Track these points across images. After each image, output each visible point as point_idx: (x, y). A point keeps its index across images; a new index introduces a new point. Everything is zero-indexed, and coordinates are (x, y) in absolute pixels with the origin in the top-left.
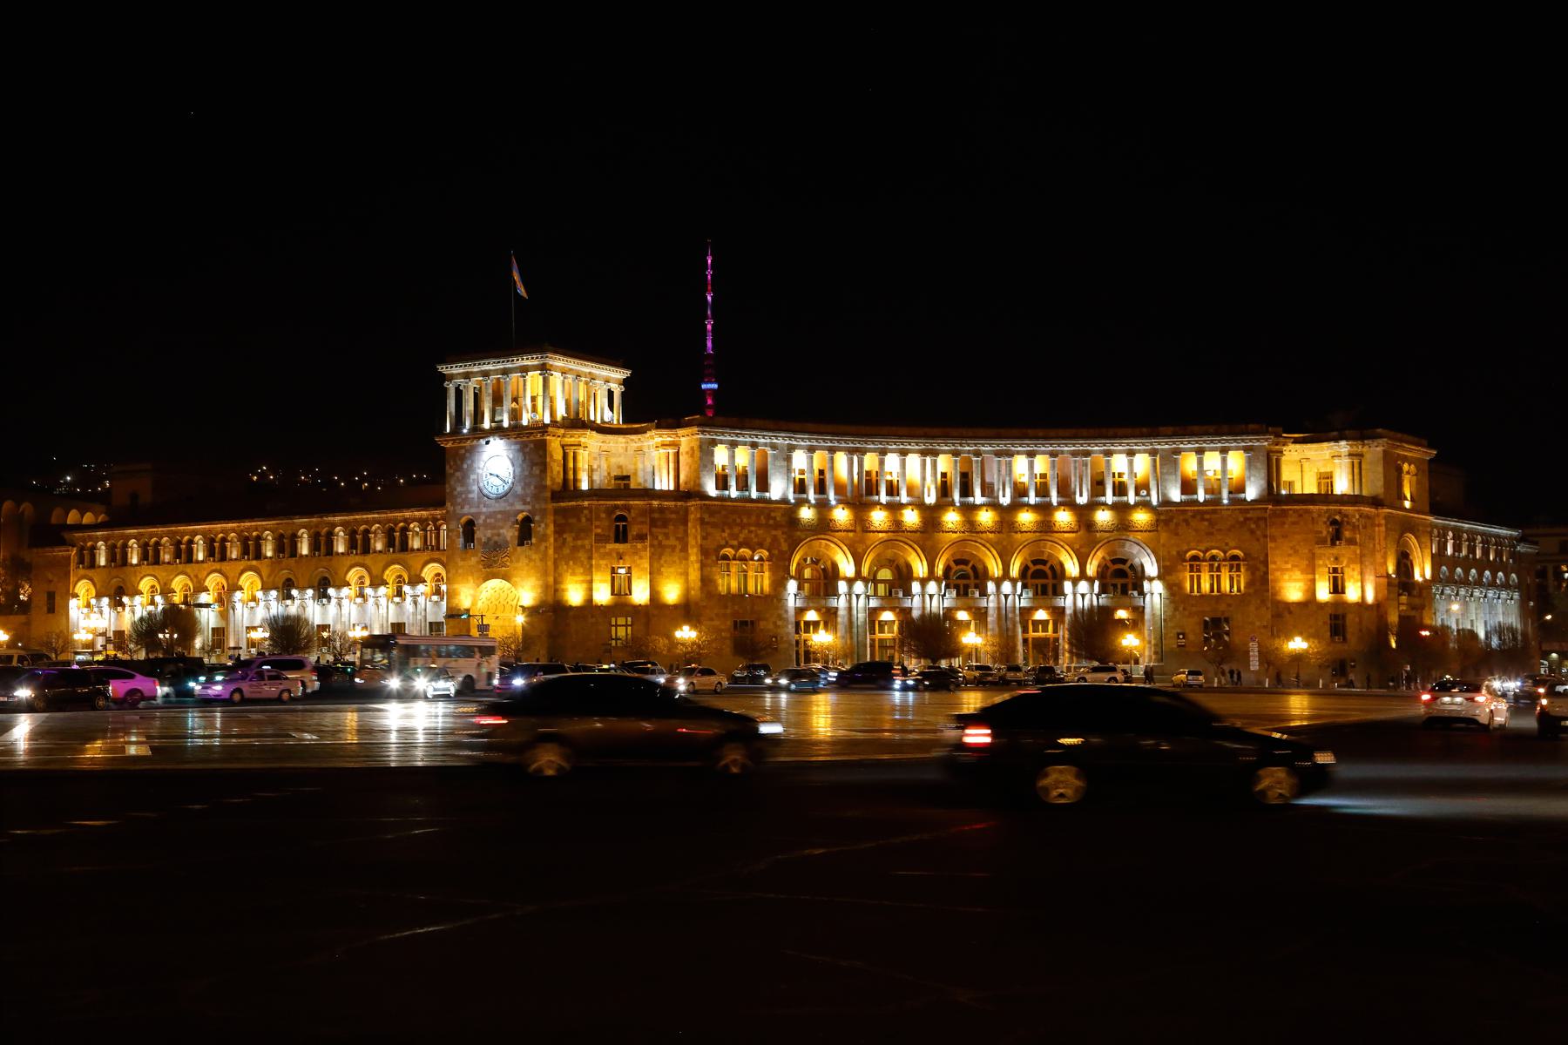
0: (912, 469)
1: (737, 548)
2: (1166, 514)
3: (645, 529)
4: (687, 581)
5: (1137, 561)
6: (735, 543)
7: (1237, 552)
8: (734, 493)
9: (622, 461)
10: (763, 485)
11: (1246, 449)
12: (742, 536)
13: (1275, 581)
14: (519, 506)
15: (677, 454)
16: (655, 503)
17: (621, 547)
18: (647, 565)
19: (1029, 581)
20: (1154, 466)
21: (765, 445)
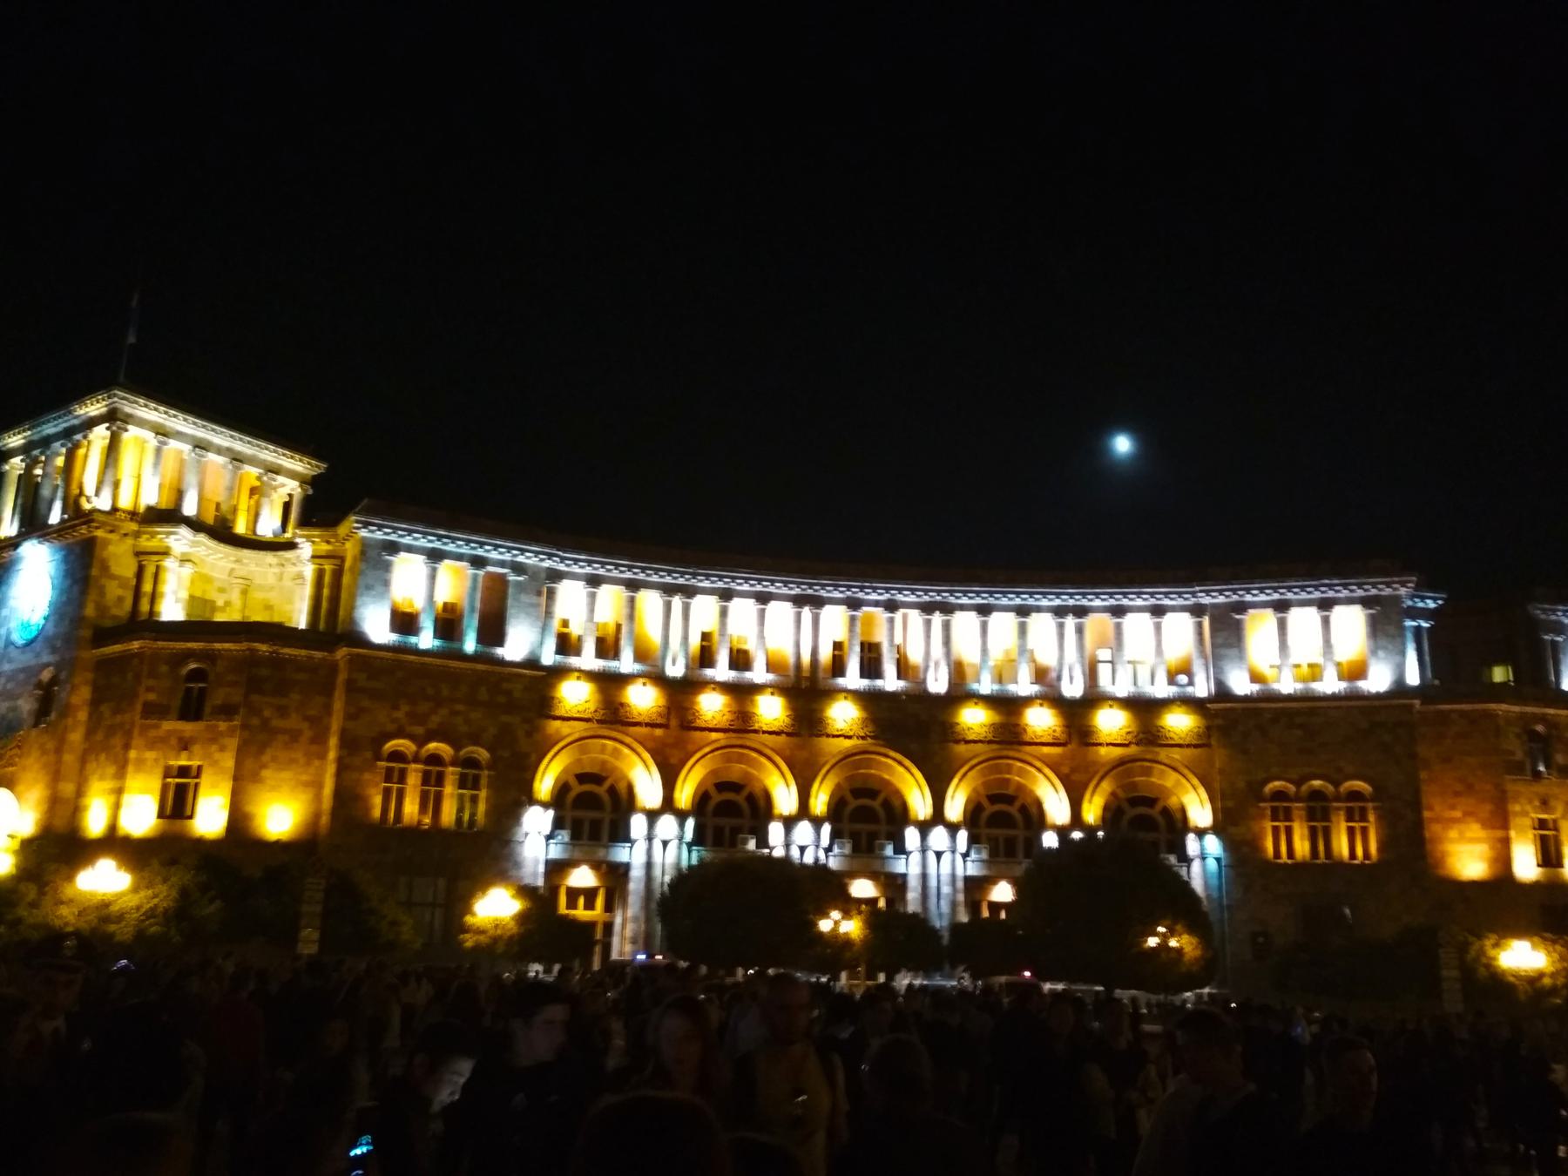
0: (771, 627)
1: (421, 742)
2: (1222, 713)
3: (236, 696)
4: (318, 798)
5: (1173, 802)
6: (419, 730)
7: (1359, 785)
8: (426, 639)
9: (273, 597)
10: (493, 631)
11: (1366, 602)
12: (435, 721)
13: (1438, 840)
14: (46, 658)
15: (338, 574)
16: (263, 648)
17: (188, 728)
18: (228, 761)
19: (984, 831)
20: (1200, 633)
21: (502, 564)
